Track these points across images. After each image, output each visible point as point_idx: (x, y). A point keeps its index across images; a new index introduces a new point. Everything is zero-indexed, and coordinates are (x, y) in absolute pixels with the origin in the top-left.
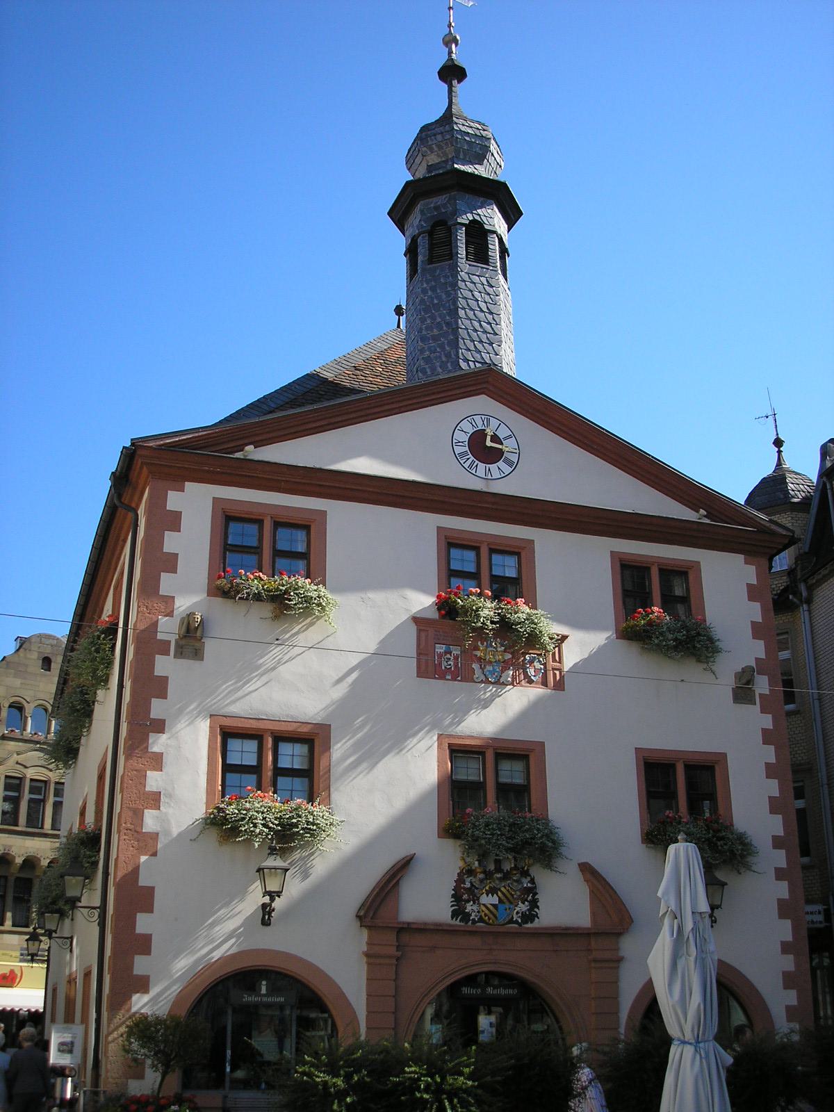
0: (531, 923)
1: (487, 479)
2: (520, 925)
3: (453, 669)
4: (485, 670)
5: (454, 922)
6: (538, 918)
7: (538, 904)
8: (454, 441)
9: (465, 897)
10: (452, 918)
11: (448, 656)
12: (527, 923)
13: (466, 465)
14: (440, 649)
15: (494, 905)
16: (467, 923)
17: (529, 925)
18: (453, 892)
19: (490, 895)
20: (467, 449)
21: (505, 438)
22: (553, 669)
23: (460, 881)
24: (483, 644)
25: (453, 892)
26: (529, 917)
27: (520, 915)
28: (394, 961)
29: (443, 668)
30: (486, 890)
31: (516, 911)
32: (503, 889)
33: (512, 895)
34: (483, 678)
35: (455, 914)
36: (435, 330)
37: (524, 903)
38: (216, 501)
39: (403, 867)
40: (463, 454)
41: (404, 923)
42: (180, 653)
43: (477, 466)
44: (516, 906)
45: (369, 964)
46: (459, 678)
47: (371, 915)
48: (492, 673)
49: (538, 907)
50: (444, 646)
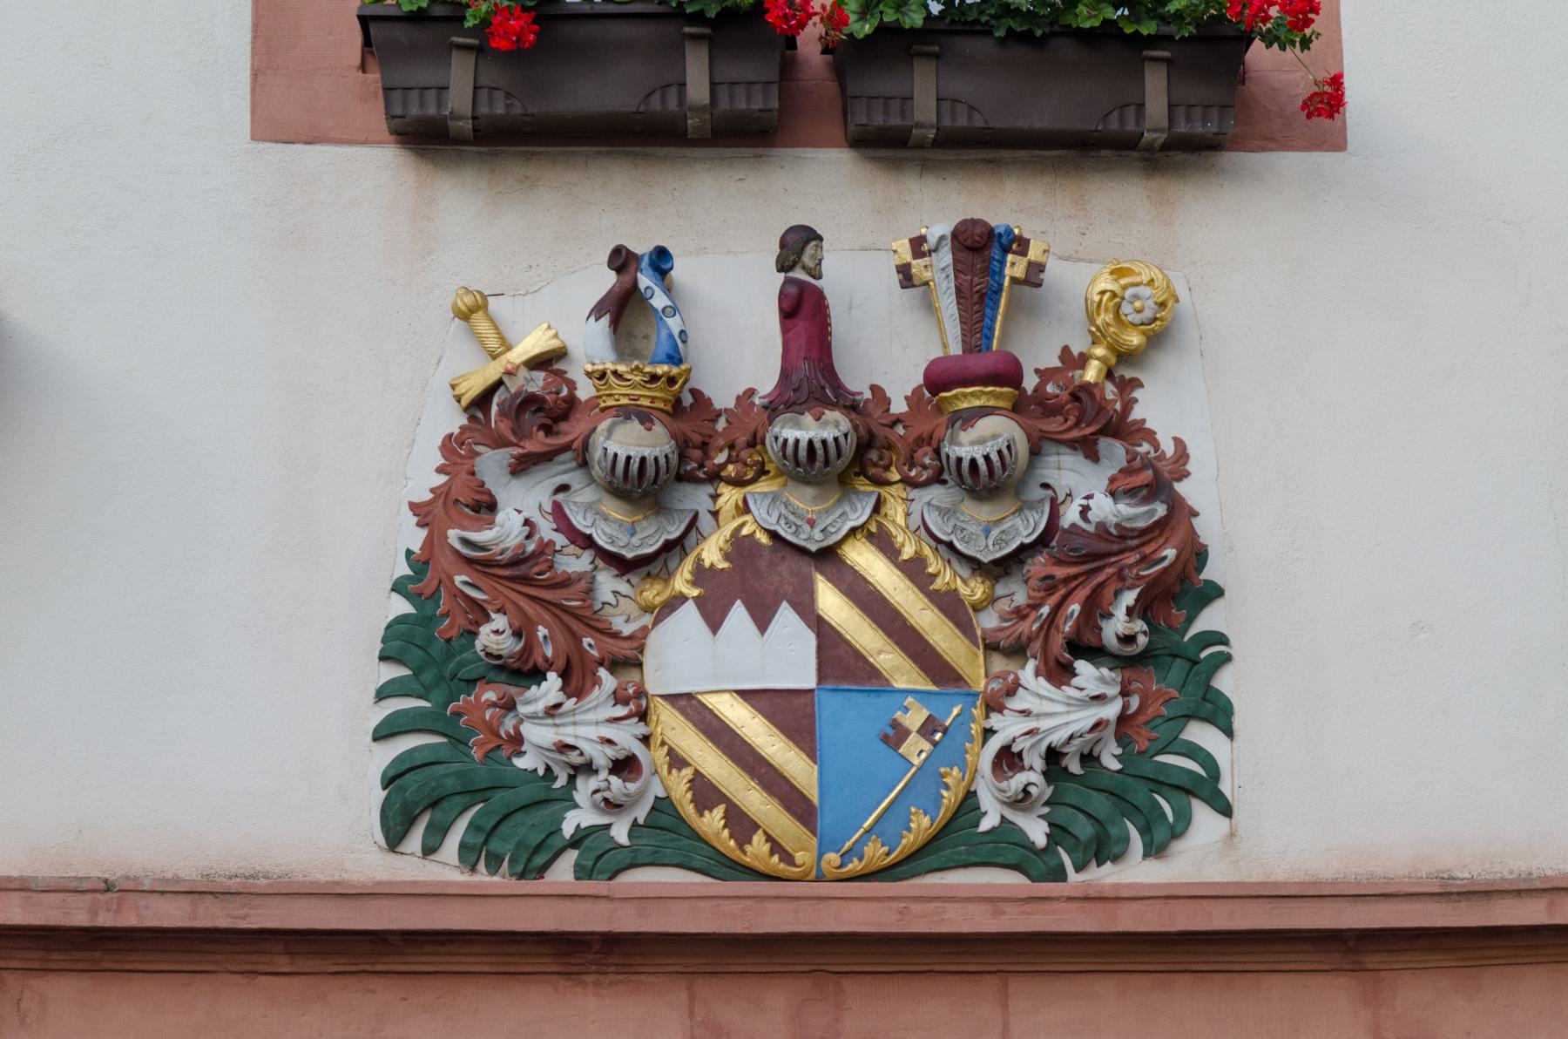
0: (1155, 850)
5: (409, 867)
6: (1225, 810)
7: (1224, 682)
10: (394, 839)
12: (1104, 849)
16: (533, 864)
18: (402, 606)
19: (738, 615)
25: (402, 606)
27: (1032, 776)
30: (702, 575)
31: (995, 744)
32: (864, 559)
33: (949, 605)
37: (1059, 673)
44: (994, 705)
49: (1220, 714)
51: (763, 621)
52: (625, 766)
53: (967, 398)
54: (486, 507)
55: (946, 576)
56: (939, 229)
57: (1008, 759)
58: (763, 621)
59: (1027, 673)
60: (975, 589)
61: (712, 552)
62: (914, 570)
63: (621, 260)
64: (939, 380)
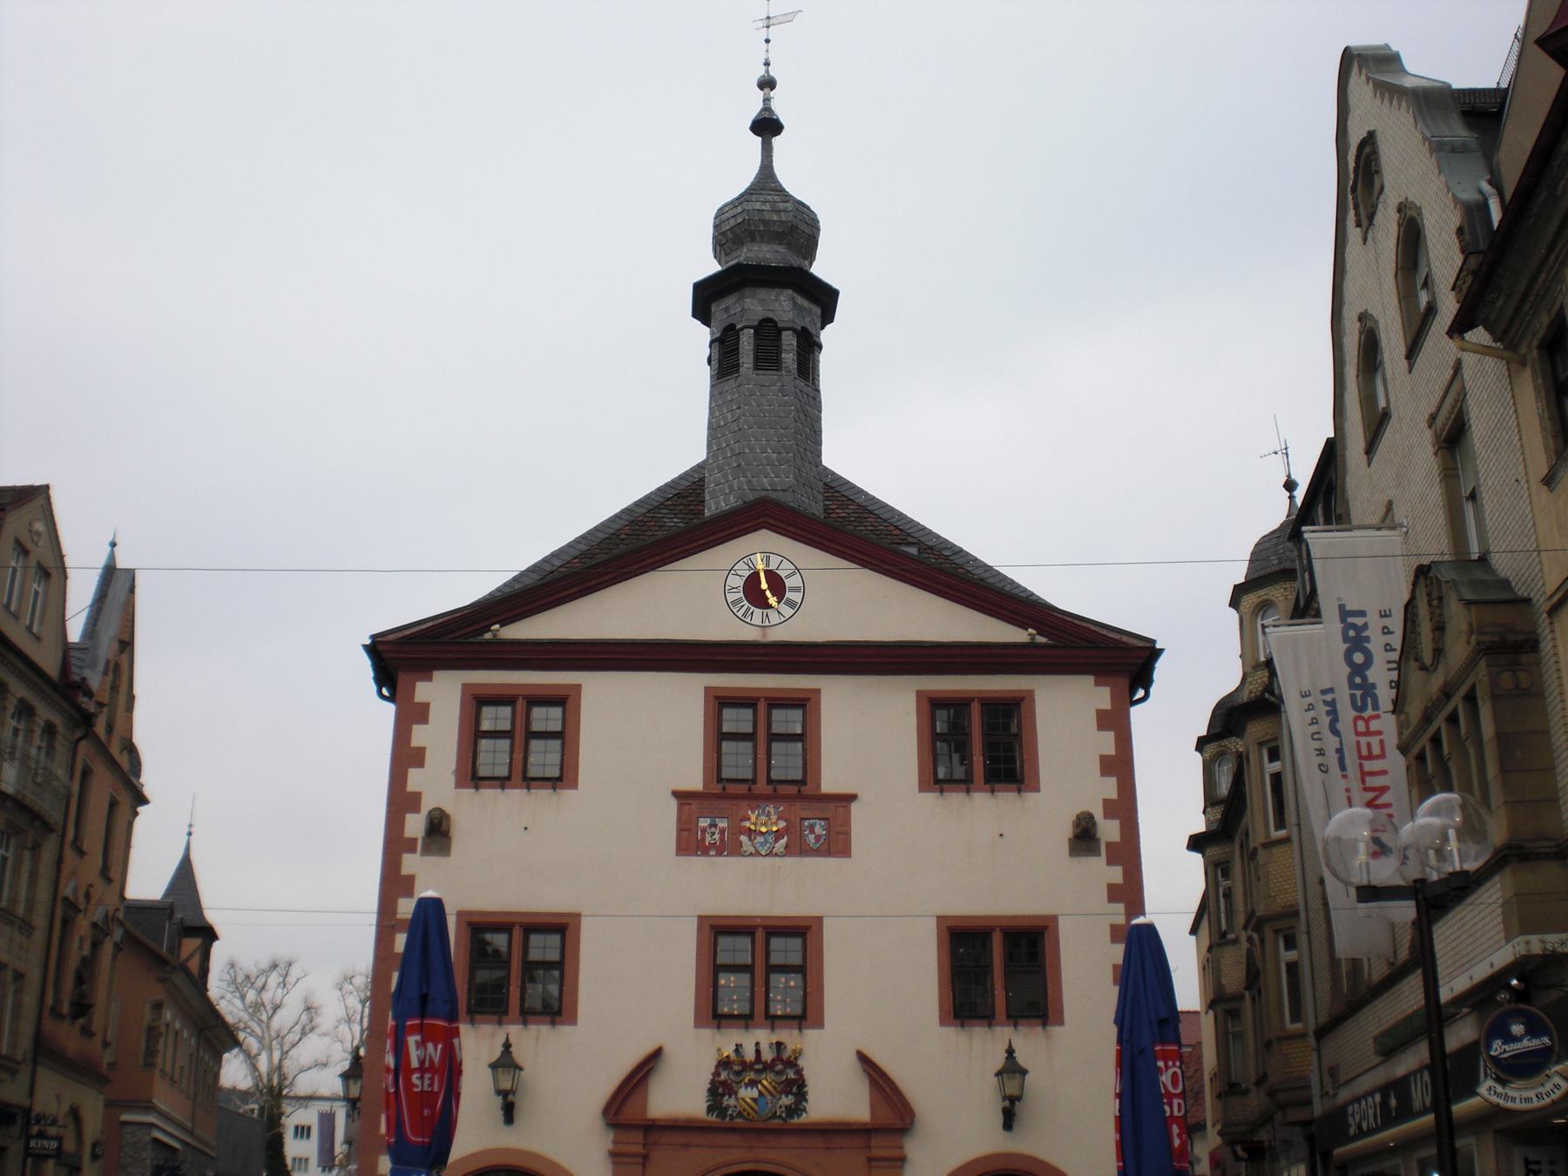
1: (764, 626)
2: (785, 1120)
3: (718, 843)
4: (755, 842)
6: (806, 1112)
8: (727, 588)
9: (720, 1090)
10: (708, 1112)
11: (713, 829)
12: (792, 1117)
13: (740, 614)
14: (704, 823)
15: (754, 1100)
16: (724, 1118)
17: (796, 1120)
18: (709, 1086)
19: (749, 1089)
20: (742, 595)
21: (787, 577)
22: (838, 833)
23: (716, 1074)
24: (753, 813)
26: (796, 1109)
27: (783, 1109)
28: (640, 1160)
29: (707, 843)
30: (745, 1084)
32: (765, 1082)
33: (775, 1088)
34: (752, 849)
35: (710, 1110)
36: (720, 458)
37: (787, 1096)
38: (465, 687)
39: (656, 1056)
40: (735, 602)
41: (649, 1120)
42: (427, 851)
43: (752, 613)
45: (614, 1163)
46: (725, 853)
47: (613, 1112)
48: (762, 844)
49: (806, 1101)
50: (709, 820)
51: (752, 1088)
52: (735, 1107)
53: (778, 1062)
54: (719, 1075)
55: (774, 1084)
56: (774, 1042)
57: (781, 1107)
58: (752, 1088)
59: (783, 1096)
60: (777, 1086)
61: (746, 1080)
62: (770, 1083)
63: (736, 1045)
64: (773, 1060)
